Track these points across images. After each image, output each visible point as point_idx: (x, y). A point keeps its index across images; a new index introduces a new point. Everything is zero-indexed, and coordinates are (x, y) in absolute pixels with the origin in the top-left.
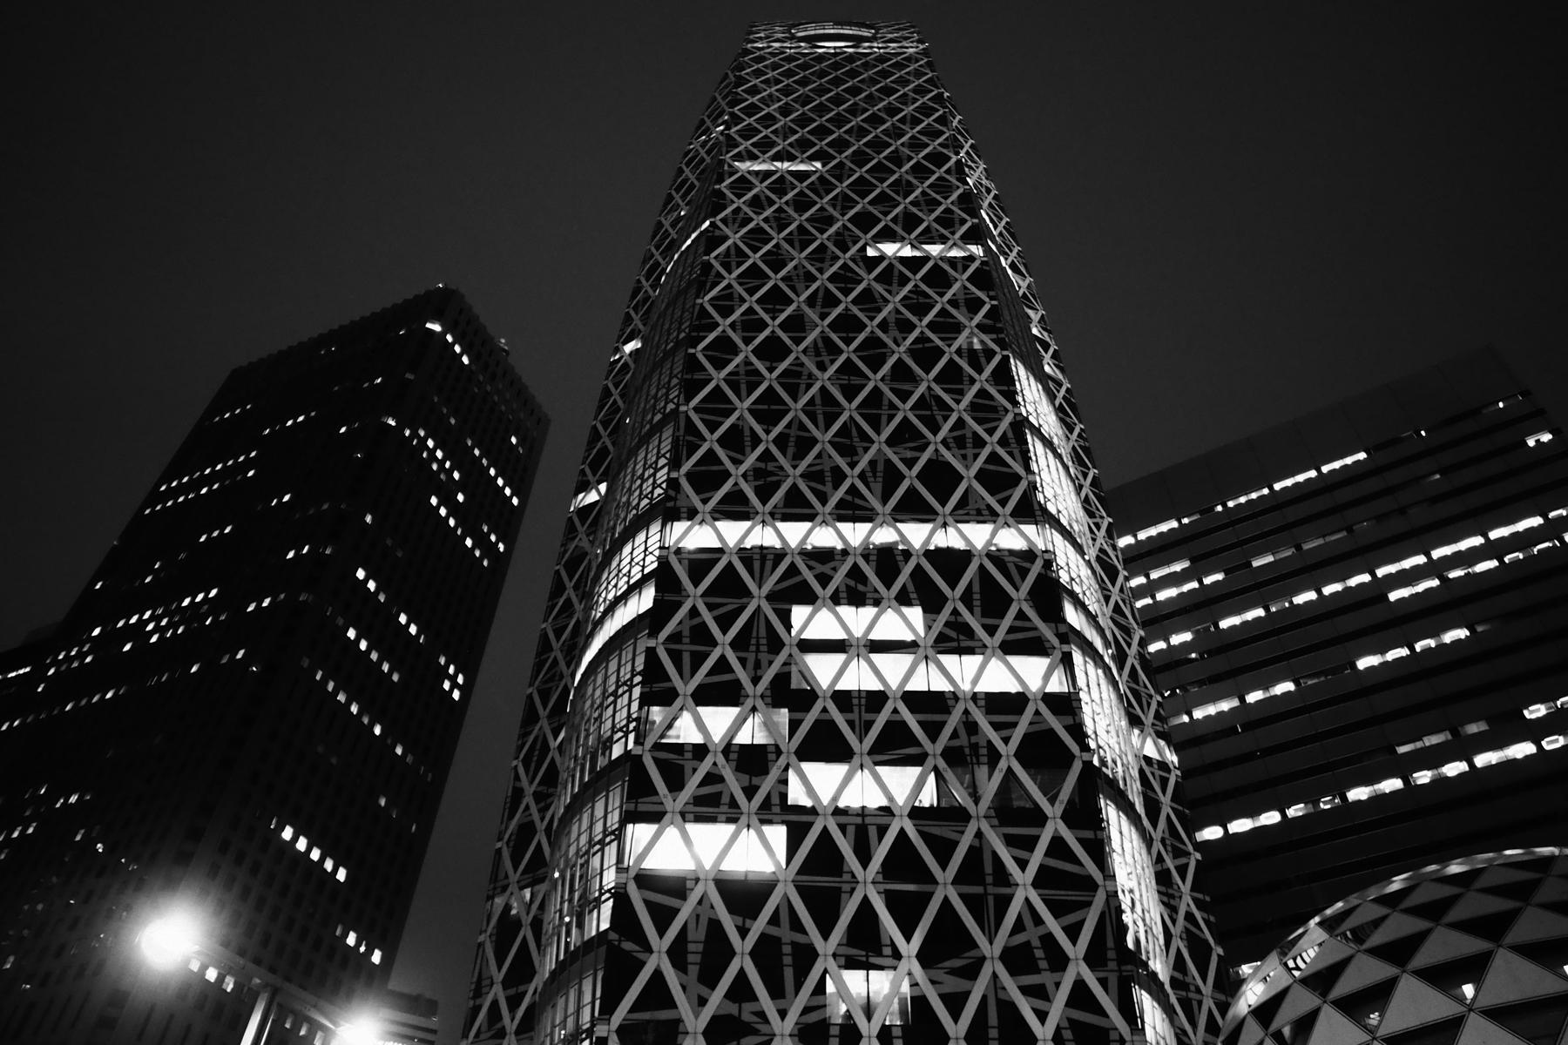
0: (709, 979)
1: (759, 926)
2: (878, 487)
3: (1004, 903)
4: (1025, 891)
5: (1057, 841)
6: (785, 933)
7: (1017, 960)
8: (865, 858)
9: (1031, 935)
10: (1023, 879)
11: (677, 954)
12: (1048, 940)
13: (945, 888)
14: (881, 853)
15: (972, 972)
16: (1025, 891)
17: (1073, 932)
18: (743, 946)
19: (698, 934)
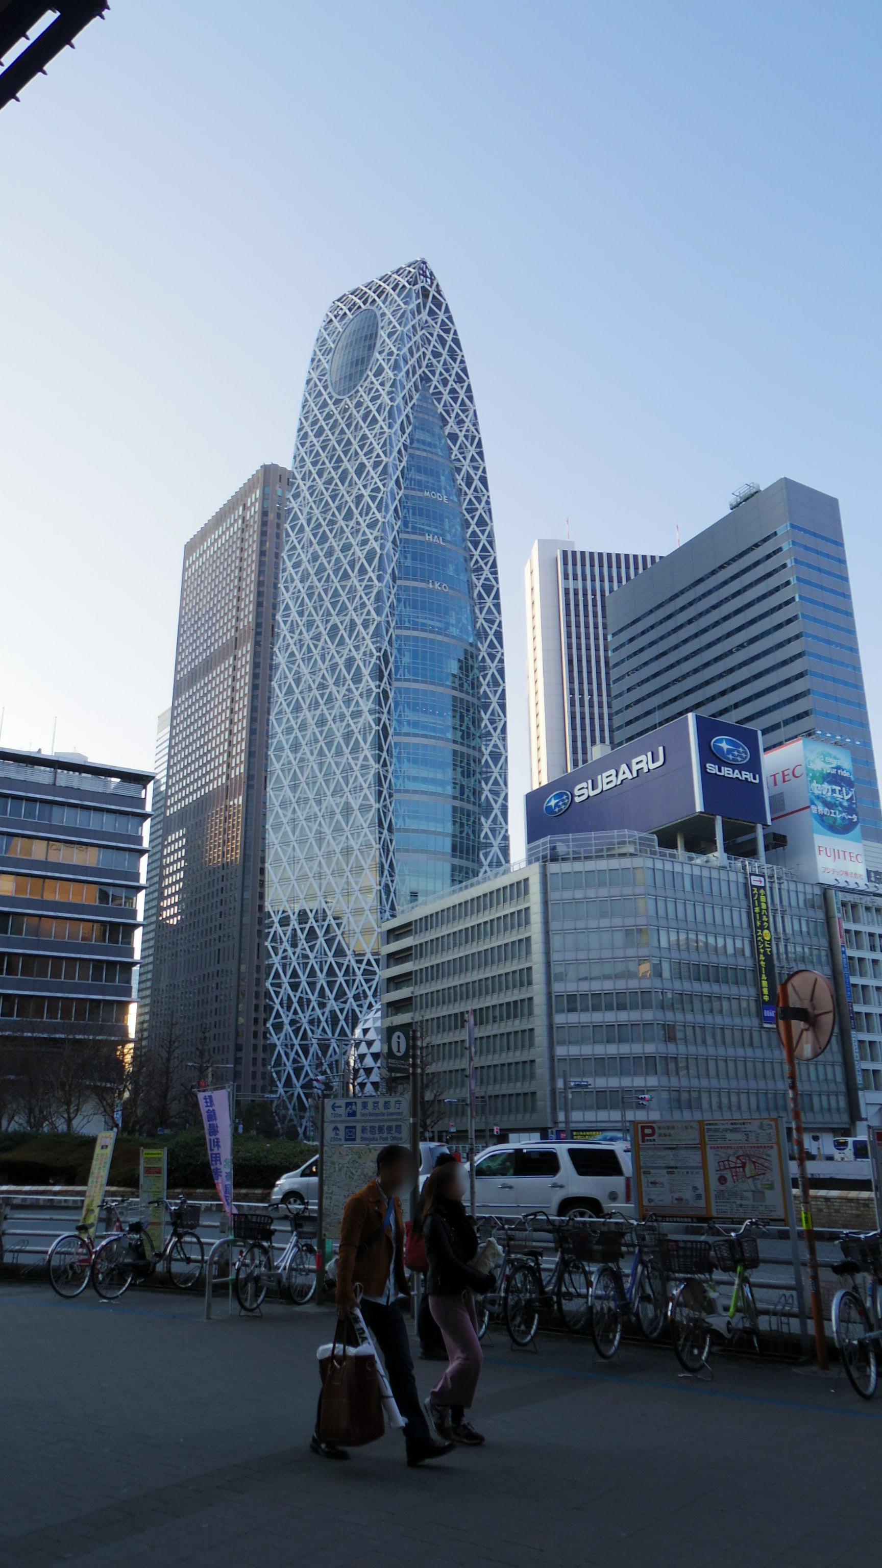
0: (288, 1010)
1: (298, 994)
3: (354, 980)
4: (360, 977)
5: (369, 960)
6: (304, 996)
7: (356, 997)
8: (321, 971)
9: (360, 990)
10: (359, 973)
11: (281, 1004)
12: (364, 991)
13: (341, 979)
14: (325, 969)
15: (345, 1002)
16: (360, 977)
17: (370, 988)
18: (295, 1000)
19: (285, 998)
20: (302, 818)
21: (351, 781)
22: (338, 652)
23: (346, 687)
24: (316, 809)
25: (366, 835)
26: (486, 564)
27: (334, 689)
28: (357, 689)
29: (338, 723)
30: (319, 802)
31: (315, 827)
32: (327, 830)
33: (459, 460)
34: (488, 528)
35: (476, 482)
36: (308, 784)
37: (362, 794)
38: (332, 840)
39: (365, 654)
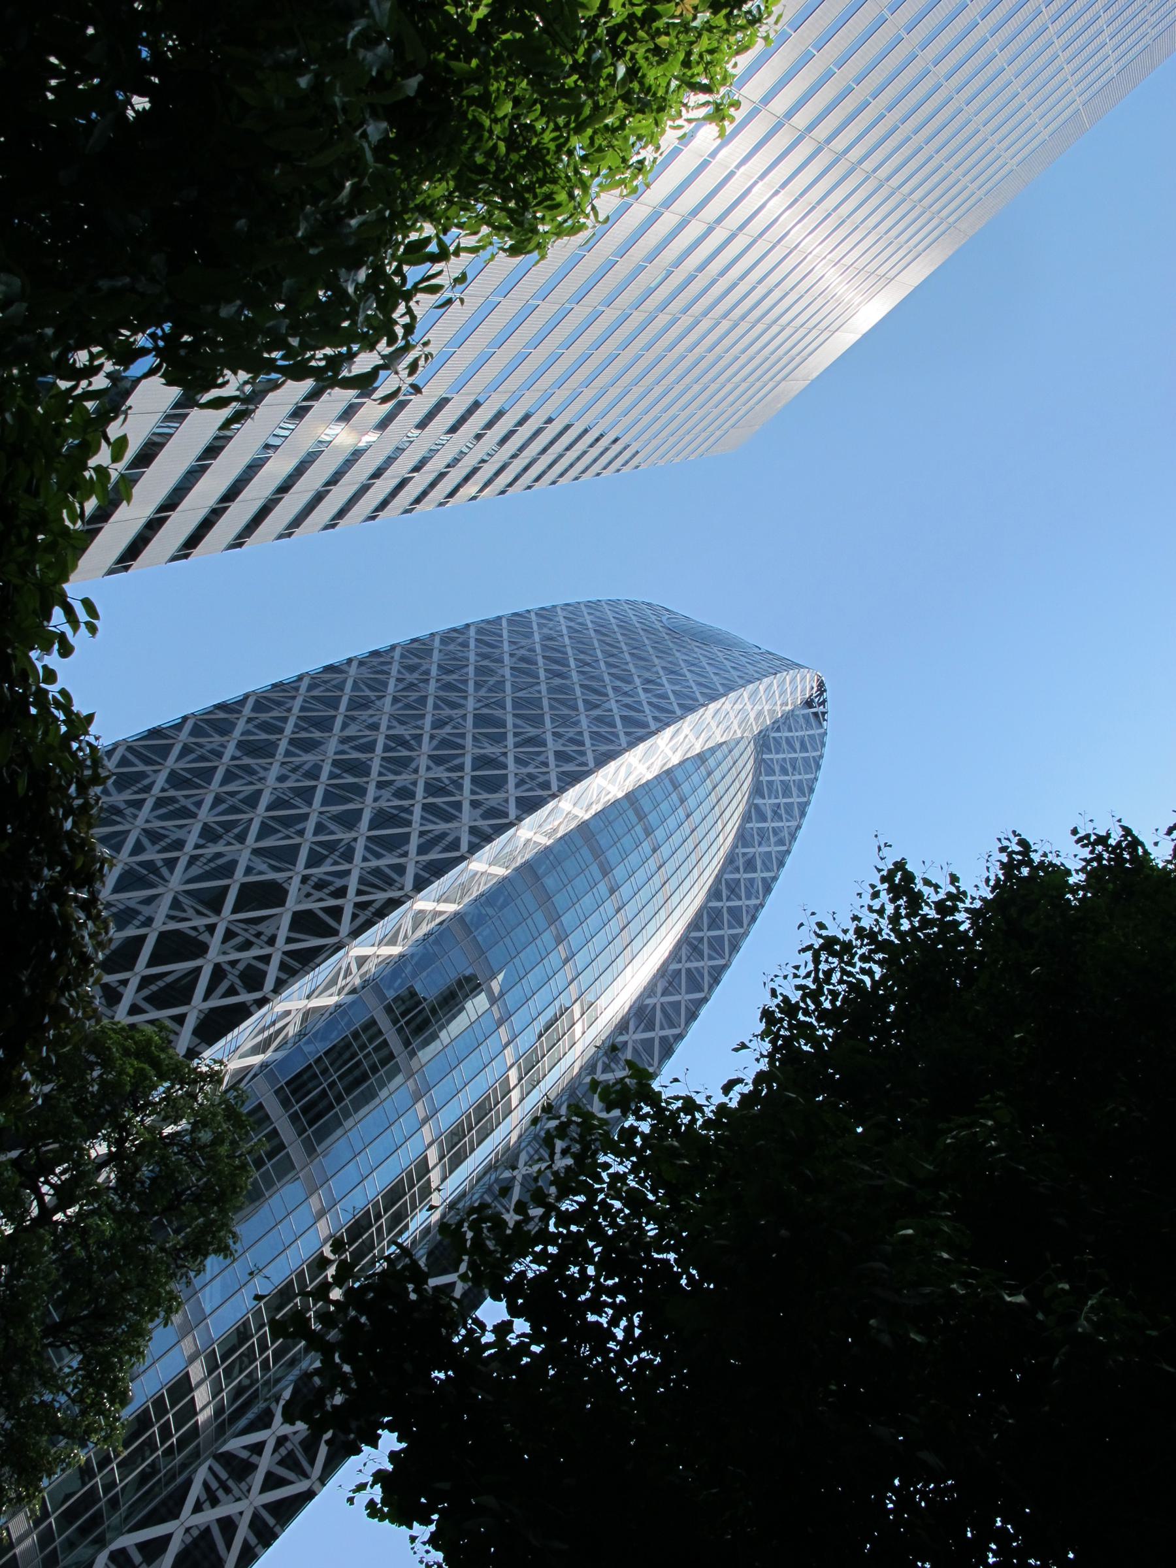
2: (195, 871)
20: (140, 822)
21: (327, 868)
22: (475, 739)
23: (454, 775)
24: (193, 839)
25: (266, 959)
26: (711, 958)
27: (423, 762)
28: (473, 792)
29: (386, 793)
30: (209, 834)
31: (151, 854)
32: (176, 881)
33: (753, 836)
34: (741, 931)
35: (758, 875)
36: (218, 800)
37: (332, 902)
38: (167, 901)
39: (531, 777)
